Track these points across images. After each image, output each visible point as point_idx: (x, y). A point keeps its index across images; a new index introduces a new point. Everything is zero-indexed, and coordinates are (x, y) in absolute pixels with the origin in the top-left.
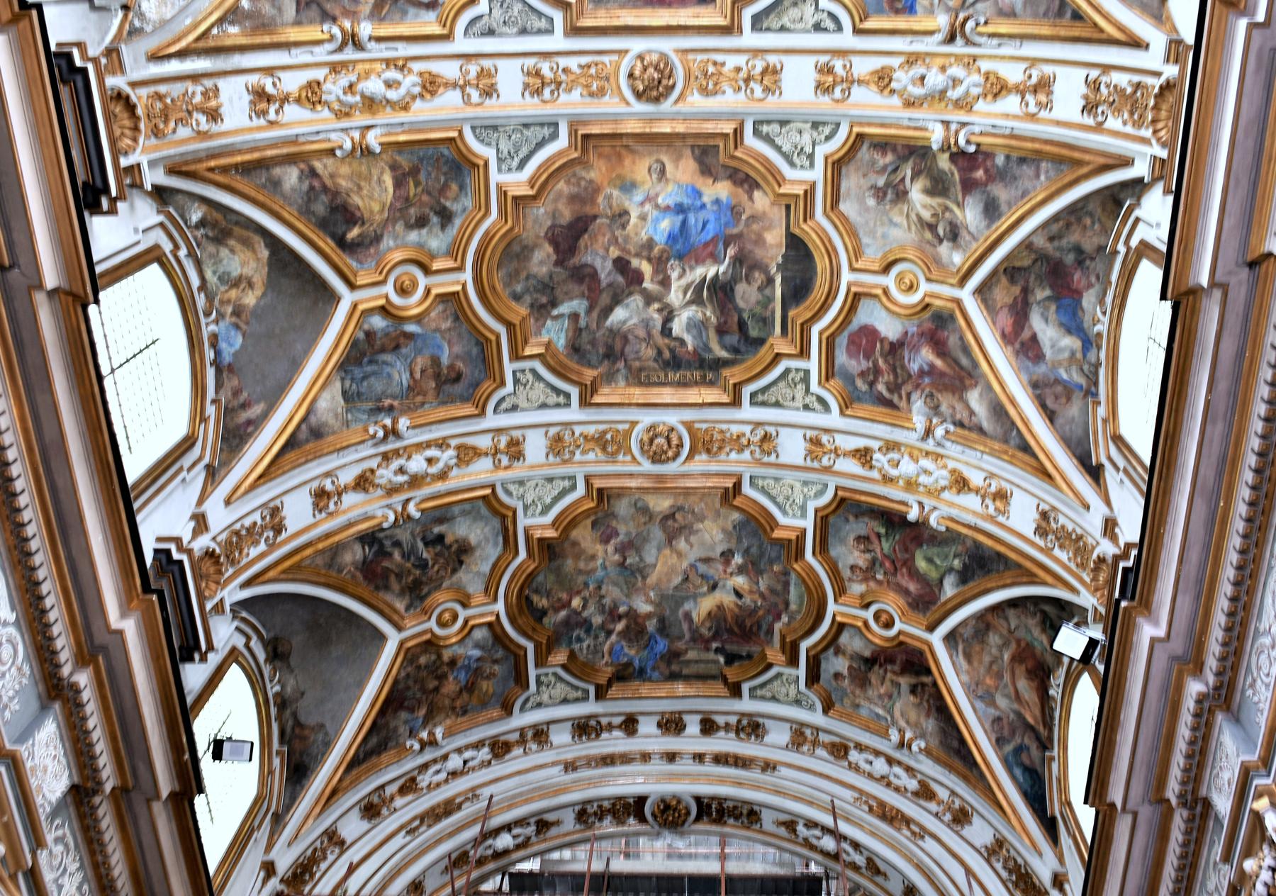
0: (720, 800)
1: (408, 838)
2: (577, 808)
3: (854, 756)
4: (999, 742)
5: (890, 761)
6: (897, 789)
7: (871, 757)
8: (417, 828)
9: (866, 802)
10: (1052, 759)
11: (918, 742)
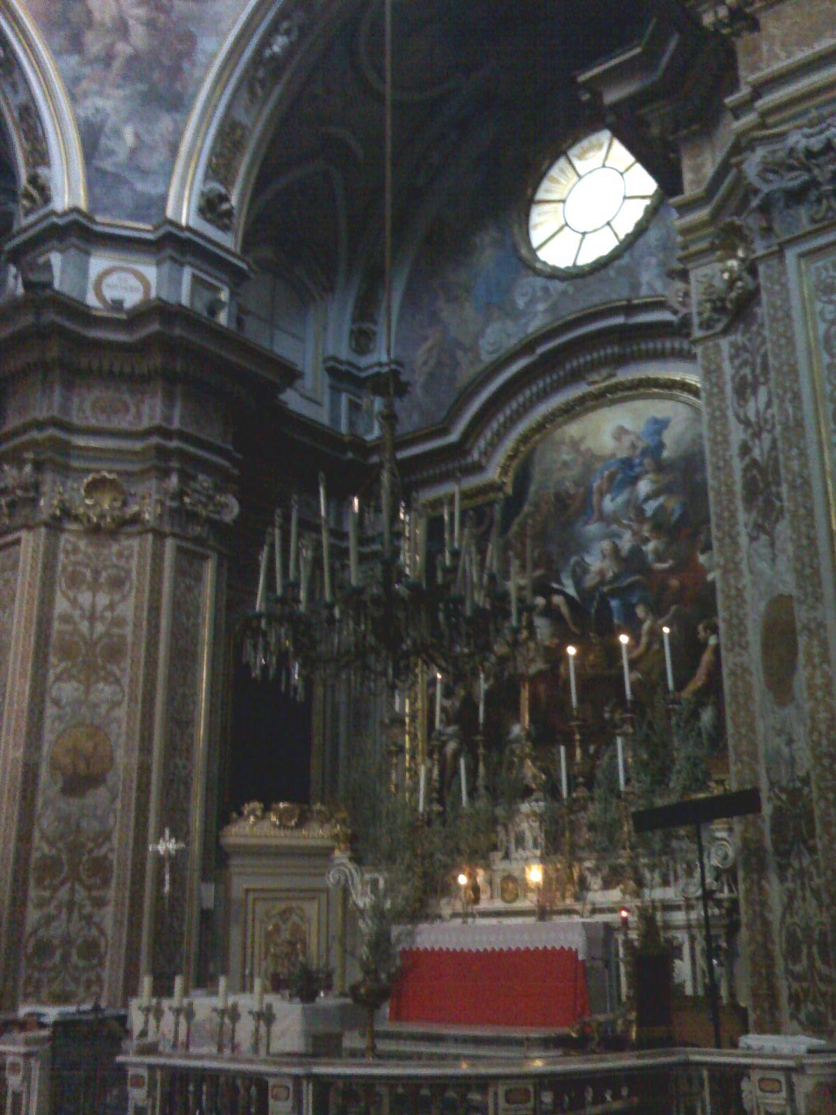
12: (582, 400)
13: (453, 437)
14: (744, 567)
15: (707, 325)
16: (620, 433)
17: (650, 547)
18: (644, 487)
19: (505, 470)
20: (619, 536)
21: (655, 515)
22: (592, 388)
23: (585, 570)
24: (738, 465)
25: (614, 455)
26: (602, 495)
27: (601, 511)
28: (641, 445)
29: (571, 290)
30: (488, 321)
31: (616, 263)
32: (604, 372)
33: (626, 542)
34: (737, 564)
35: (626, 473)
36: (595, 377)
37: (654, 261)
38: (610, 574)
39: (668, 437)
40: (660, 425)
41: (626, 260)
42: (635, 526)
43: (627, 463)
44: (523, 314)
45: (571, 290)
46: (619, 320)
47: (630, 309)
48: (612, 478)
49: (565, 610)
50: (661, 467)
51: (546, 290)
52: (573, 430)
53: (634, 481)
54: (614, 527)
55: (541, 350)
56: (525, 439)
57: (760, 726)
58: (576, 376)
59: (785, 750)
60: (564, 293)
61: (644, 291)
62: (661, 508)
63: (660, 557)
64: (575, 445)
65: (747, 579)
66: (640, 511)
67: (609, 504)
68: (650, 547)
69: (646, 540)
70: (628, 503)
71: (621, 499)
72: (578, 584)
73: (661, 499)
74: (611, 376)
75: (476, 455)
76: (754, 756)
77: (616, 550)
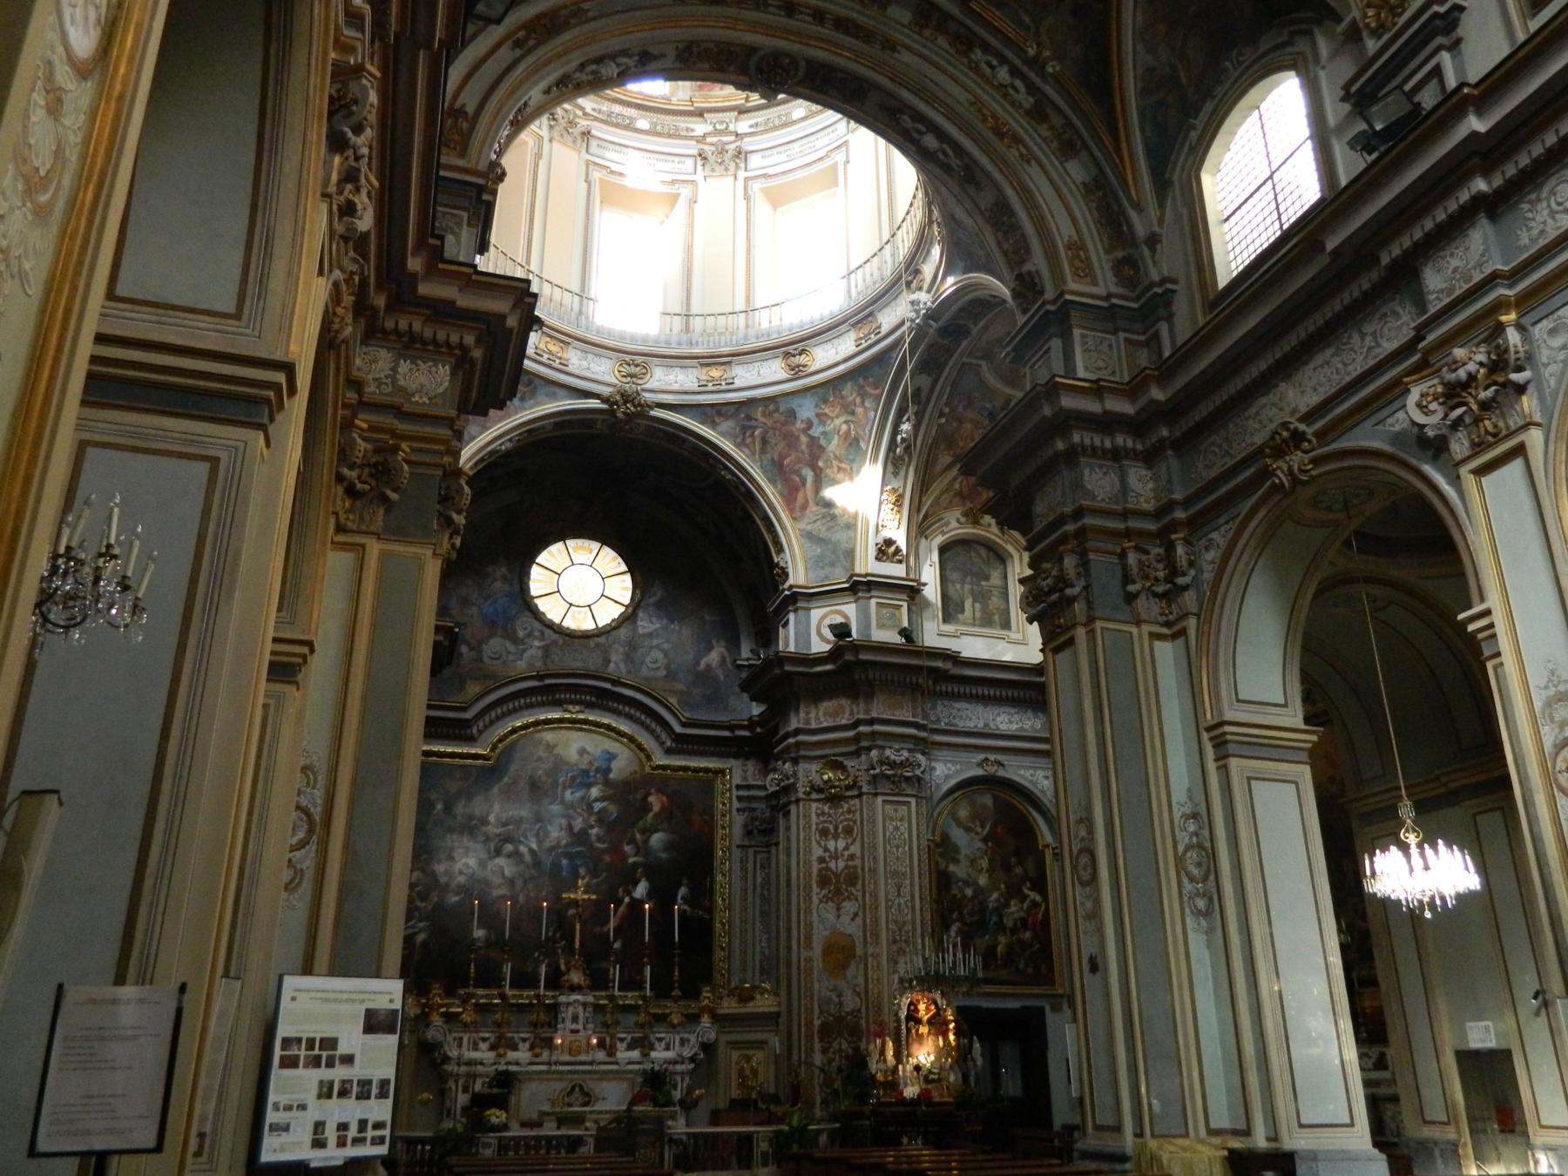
0: (833, 69)
1: (518, 52)
2: (681, 46)
3: (978, 55)
4: (1143, 92)
5: (1014, 72)
6: (1012, 104)
7: (995, 62)
8: (526, 39)
9: (980, 111)
10: (1193, 127)
11: (1054, 63)
12: (561, 721)
13: (468, 715)
14: (814, 911)
15: (809, 794)
16: (582, 752)
17: (594, 831)
18: (595, 792)
19: (494, 747)
20: (574, 819)
21: (599, 812)
22: (568, 716)
23: (547, 835)
24: (815, 867)
25: (576, 765)
26: (565, 788)
27: (563, 798)
28: (596, 764)
29: (561, 642)
30: (491, 636)
31: (596, 639)
32: (577, 708)
33: (578, 824)
34: (811, 911)
35: (583, 779)
36: (571, 707)
37: (621, 650)
38: (564, 842)
39: (615, 765)
40: (611, 757)
41: (602, 640)
42: (586, 815)
43: (585, 773)
44: (522, 642)
45: (561, 642)
46: (608, 686)
47: (615, 682)
48: (573, 779)
49: (528, 858)
50: (607, 783)
51: (542, 633)
52: (549, 736)
53: (589, 786)
54: (571, 812)
55: (548, 682)
56: (514, 731)
57: (817, 985)
58: (558, 704)
59: (837, 1000)
60: (555, 642)
61: (612, 665)
62: (603, 810)
63: (599, 839)
64: (550, 747)
65: (815, 918)
66: (590, 807)
67: (568, 795)
68: (594, 831)
69: (592, 827)
70: (582, 798)
71: (578, 795)
72: (540, 841)
73: (605, 804)
74: (582, 712)
75: (475, 731)
76: (812, 998)
77: (570, 827)
